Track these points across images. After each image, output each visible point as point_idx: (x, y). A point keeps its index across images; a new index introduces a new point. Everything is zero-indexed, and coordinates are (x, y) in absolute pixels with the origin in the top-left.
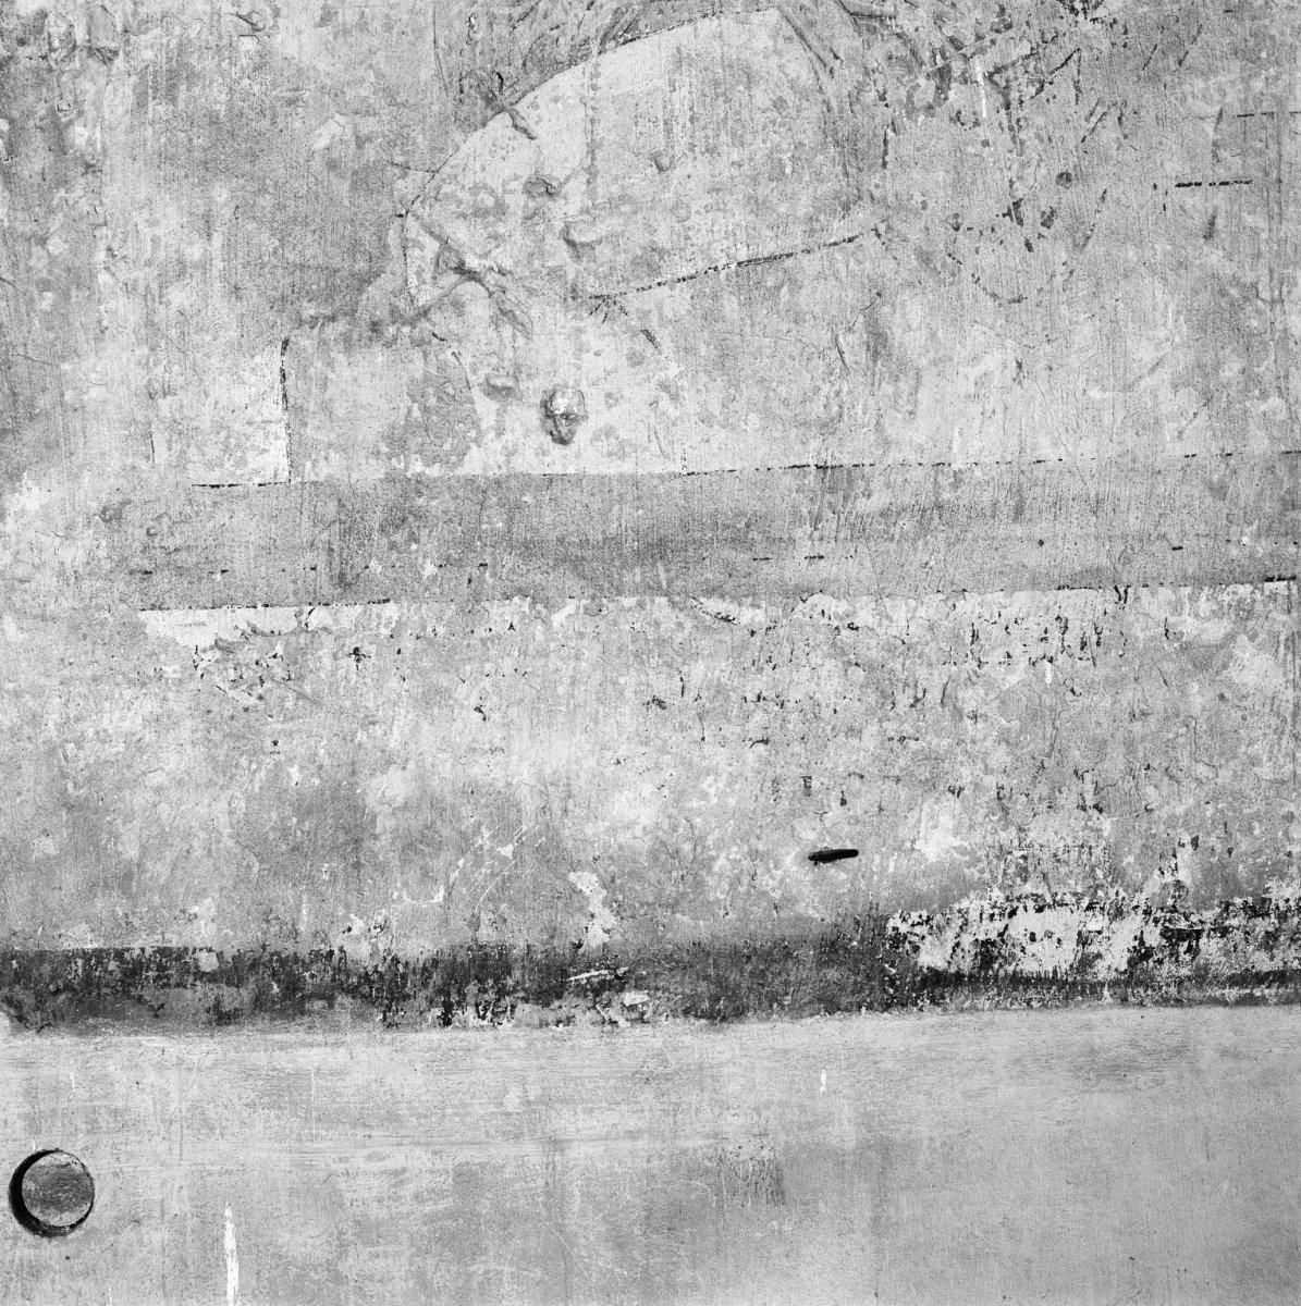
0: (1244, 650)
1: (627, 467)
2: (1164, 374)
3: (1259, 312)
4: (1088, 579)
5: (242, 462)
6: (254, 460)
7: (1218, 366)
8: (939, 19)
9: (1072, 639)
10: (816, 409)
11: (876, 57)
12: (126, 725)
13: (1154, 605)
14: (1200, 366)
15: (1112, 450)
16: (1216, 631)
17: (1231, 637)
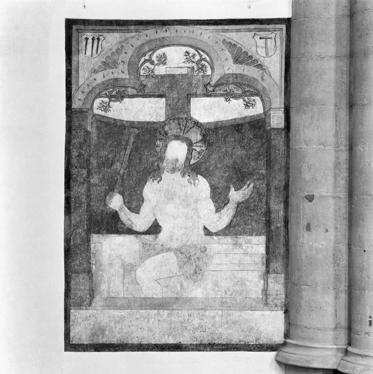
0: (216, 317)
1: (157, 297)
2: (210, 289)
3: (219, 284)
4: (202, 309)
5: (119, 295)
6: (120, 295)
7: (215, 289)
8: (189, 254)
10: (176, 292)
11: (183, 257)
12: (106, 321)
14: (213, 289)
15: (205, 297)
16: (214, 315)
17: (215, 316)
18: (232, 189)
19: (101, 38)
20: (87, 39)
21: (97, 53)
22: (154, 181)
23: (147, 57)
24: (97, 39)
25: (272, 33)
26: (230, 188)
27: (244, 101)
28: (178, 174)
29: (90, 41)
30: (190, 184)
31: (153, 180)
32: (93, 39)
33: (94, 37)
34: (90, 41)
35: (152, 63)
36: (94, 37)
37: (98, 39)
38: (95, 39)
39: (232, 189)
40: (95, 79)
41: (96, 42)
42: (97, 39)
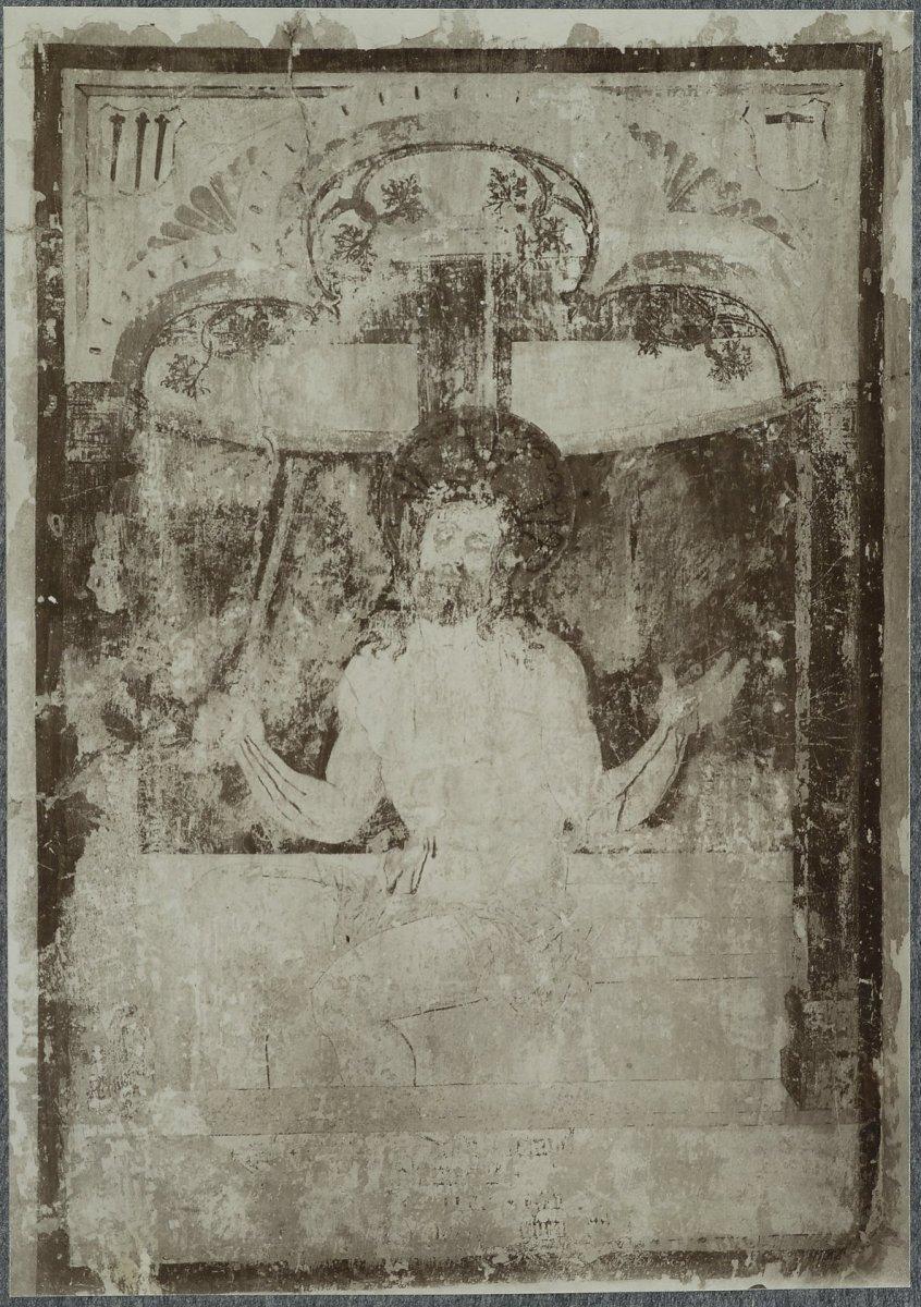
9: (554, 1146)
13: (582, 1136)
18: (669, 682)
19: (175, 120)
20: (118, 120)
21: (157, 177)
22: (378, 652)
23: (345, 192)
24: (157, 120)
25: (812, 101)
26: (659, 681)
27: (710, 353)
28: (468, 627)
29: (129, 130)
30: (512, 662)
31: (374, 652)
32: (142, 121)
33: (143, 115)
34: (129, 130)
35: (366, 211)
36: (143, 115)
37: (162, 122)
38: (148, 121)
39: (669, 682)
40: (150, 272)
41: (152, 129)
42: (157, 120)
